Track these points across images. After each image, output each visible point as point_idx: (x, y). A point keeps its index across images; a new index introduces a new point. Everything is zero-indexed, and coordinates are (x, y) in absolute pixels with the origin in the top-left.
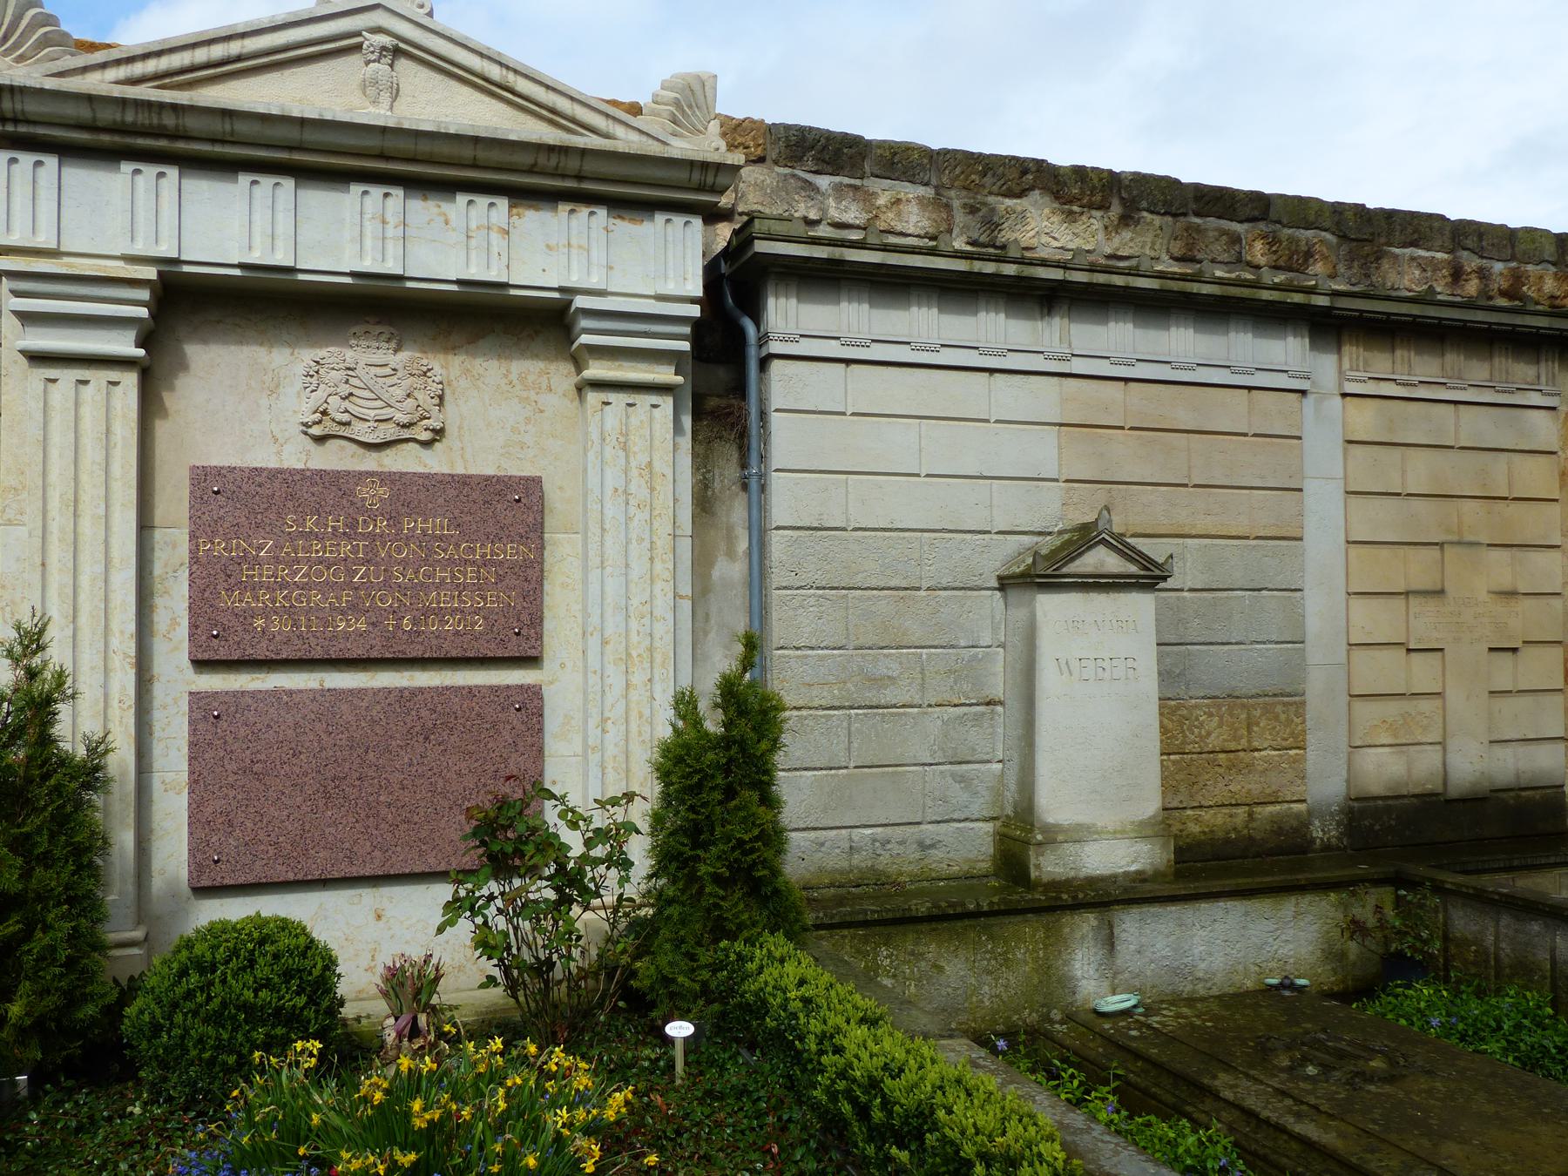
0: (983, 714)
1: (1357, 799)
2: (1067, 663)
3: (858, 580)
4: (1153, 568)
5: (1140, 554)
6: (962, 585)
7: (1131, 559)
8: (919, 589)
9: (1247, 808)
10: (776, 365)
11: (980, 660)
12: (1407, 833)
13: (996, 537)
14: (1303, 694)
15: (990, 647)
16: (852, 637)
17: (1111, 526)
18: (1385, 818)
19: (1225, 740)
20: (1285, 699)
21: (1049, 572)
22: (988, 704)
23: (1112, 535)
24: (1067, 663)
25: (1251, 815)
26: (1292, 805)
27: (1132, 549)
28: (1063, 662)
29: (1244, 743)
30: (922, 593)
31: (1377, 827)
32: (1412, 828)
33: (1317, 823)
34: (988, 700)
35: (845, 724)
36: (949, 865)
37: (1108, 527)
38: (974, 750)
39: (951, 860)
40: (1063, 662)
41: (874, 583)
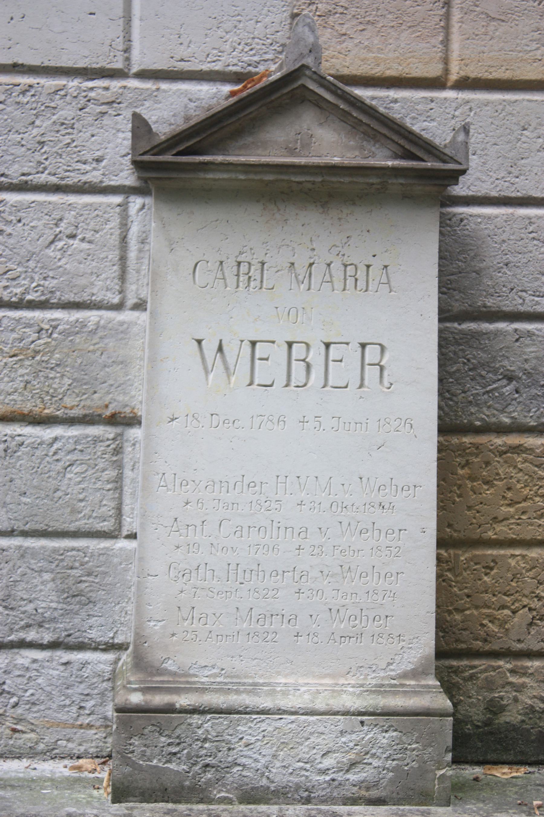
0: (96, 440)
2: (220, 349)
4: (420, 154)
6: (53, 180)
11: (93, 332)
13: (134, 83)
15: (119, 307)
17: (318, 61)
21: (168, 158)
23: (321, 80)
24: (220, 349)
28: (210, 348)
34: (108, 413)
36: (14, 731)
37: (309, 61)
38: (74, 511)
39: (19, 720)
40: (210, 348)
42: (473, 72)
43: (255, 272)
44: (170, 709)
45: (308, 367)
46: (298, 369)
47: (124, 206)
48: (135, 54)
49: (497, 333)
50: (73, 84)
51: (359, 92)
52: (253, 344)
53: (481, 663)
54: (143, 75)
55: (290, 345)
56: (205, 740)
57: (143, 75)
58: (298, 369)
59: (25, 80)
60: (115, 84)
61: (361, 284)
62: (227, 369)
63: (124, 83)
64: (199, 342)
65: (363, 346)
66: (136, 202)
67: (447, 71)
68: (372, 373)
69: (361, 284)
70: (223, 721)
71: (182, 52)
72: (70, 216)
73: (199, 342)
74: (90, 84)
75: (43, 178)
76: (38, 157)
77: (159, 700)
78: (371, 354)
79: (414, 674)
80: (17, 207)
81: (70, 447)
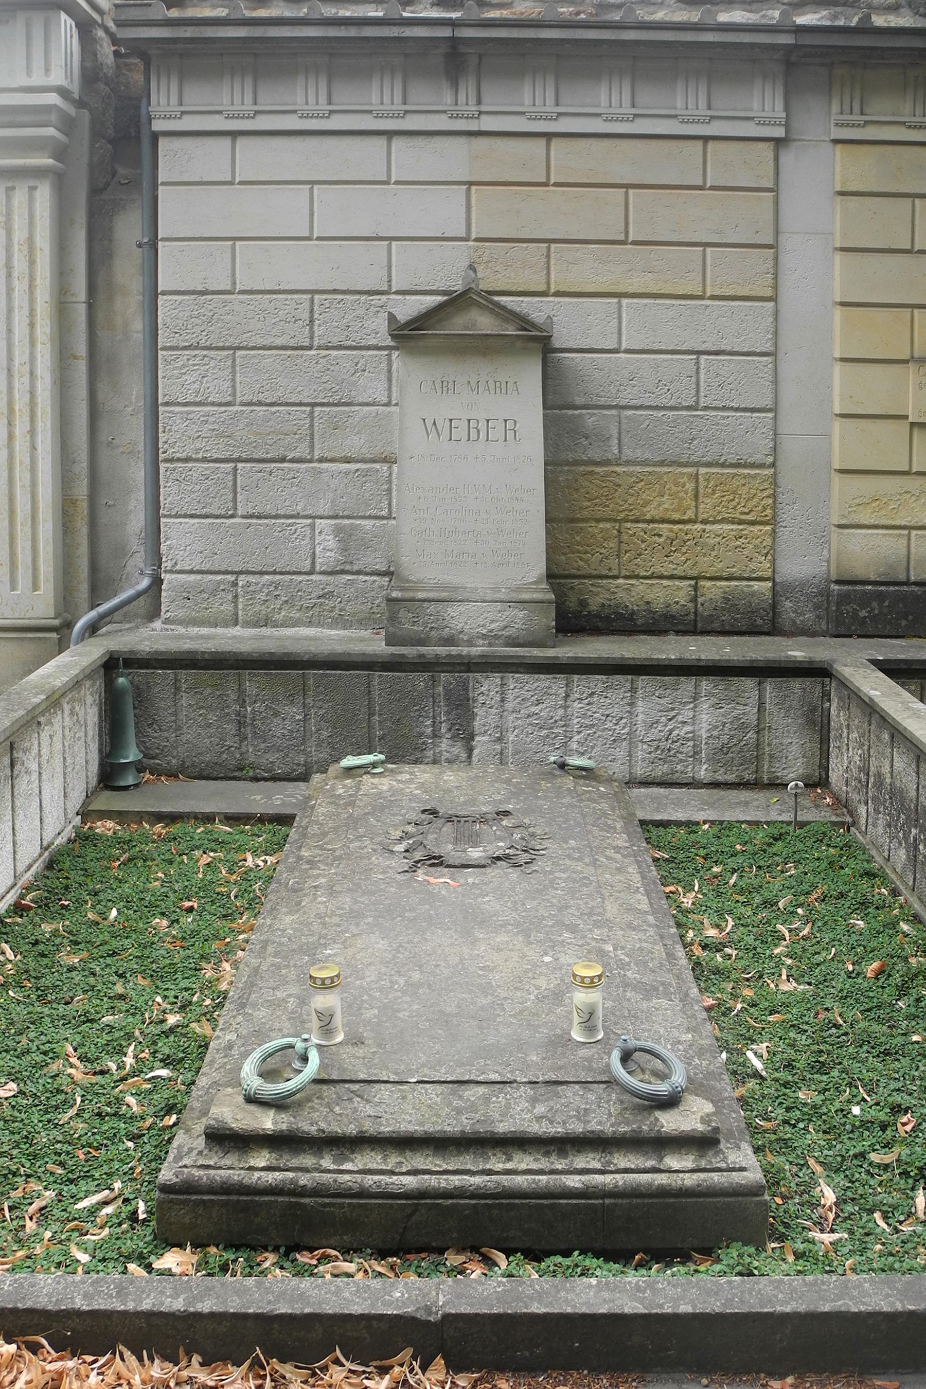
1: (838, 582)
2: (434, 423)
3: (244, 340)
5: (512, 312)
7: (506, 320)
8: (310, 348)
9: (693, 582)
10: (163, 143)
12: (904, 623)
14: (773, 465)
16: (238, 395)
17: (477, 285)
18: (875, 604)
19: (667, 510)
20: (746, 471)
22: (385, 460)
23: (479, 295)
24: (434, 423)
25: (696, 588)
26: (752, 583)
27: (504, 308)
28: (429, 423)
29: (690, 514)
30: (313, 352)
31: (863, 613)
32: (910, 618)
33: (788, 604)
35: (230, 478)
37: (473, 286)
40: (429, 423)
41: (260, 341)
42: (562, 288)
43: (451, 386)
44: (413, 600)
45: (478, 431)
46: (473, 433)
47: (389, 355)
48: (394, 283)
49: (580, 415)
50: (363, 298)
51: (503, 300)
52: (451, 420)
53: (576, 582)
54: (397, 293)
55: (469, 421)
56: (431, 615)
57: (397, 293)
58: (473, 433)
59: (340, 297)
60: (384, 298)
61: (504, 391)
62: (438, 433)
63: (388, 297)
64: (424, 420)
65: (506, 421)
66: (395, 354)
67: (549, 288)
68: (510, 434)
69: (504, 391)
70: (440, 606)
71: (416, 281)
72: (362, 362)
73: (424, 420)
74: (372, 298)
75: (349, 343)
76: (346, 333)
77: (409, 595)
78: (510, 425)
79: (535, 583)
80: (336, 358)
81: (364, 473)
